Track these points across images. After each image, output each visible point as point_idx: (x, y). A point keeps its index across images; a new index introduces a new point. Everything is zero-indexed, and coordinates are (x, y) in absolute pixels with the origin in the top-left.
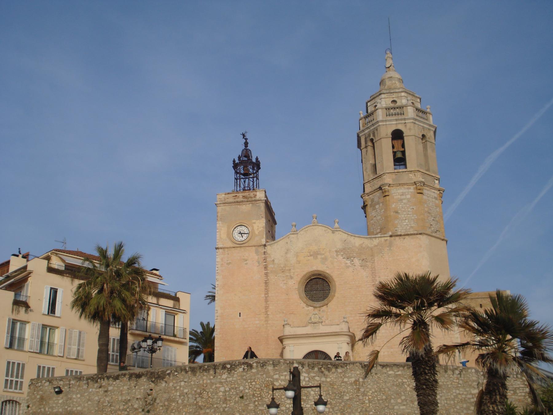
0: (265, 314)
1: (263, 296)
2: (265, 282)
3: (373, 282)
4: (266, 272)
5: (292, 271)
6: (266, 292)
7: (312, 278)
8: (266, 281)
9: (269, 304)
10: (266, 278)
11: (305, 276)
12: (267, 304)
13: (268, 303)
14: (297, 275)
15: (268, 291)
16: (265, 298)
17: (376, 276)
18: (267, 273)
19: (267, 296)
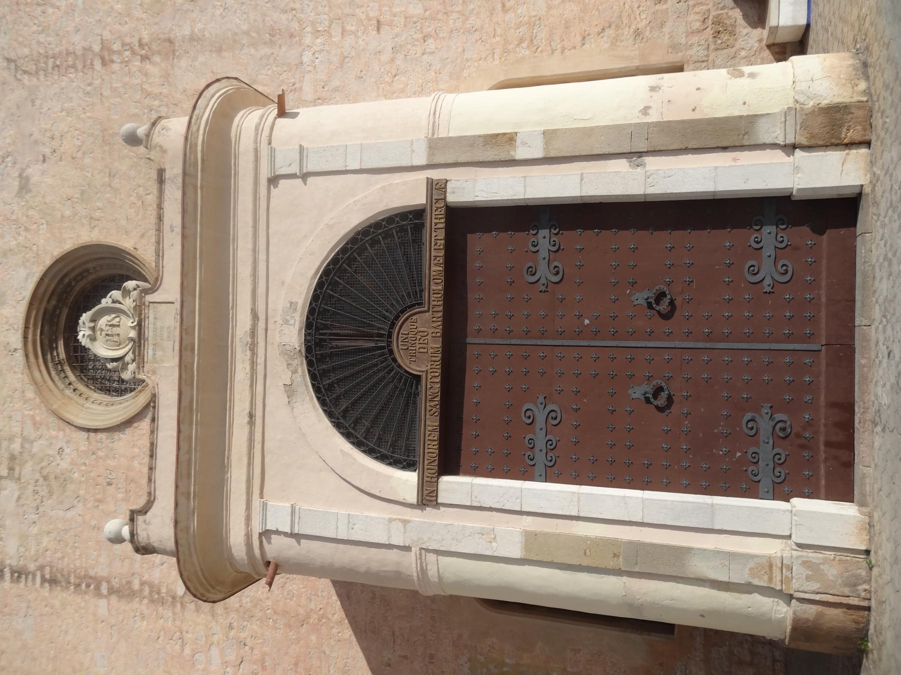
0: (183, 606)
1: (103, 603)
2: (47, 585)
3: (92, 64)
4: (7, 575)
5: (16, 446)
6: (88, 586)
7: (63, 355)
8: (44, 580)
9: (143, 583)
10: (34, 576)
11: (39, 390)
12: (141, 591)
13: (136, 586)
14: (36, 425)
15: (86, 576)
16: (114, 599)
17: (68, 53)
18: (12, 572)
19: (104, 589)
